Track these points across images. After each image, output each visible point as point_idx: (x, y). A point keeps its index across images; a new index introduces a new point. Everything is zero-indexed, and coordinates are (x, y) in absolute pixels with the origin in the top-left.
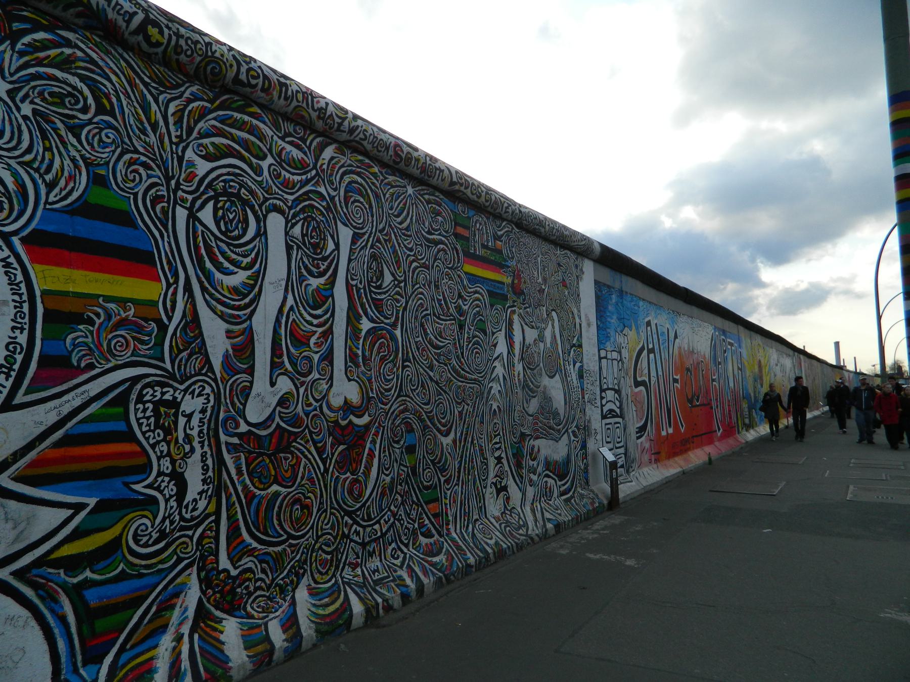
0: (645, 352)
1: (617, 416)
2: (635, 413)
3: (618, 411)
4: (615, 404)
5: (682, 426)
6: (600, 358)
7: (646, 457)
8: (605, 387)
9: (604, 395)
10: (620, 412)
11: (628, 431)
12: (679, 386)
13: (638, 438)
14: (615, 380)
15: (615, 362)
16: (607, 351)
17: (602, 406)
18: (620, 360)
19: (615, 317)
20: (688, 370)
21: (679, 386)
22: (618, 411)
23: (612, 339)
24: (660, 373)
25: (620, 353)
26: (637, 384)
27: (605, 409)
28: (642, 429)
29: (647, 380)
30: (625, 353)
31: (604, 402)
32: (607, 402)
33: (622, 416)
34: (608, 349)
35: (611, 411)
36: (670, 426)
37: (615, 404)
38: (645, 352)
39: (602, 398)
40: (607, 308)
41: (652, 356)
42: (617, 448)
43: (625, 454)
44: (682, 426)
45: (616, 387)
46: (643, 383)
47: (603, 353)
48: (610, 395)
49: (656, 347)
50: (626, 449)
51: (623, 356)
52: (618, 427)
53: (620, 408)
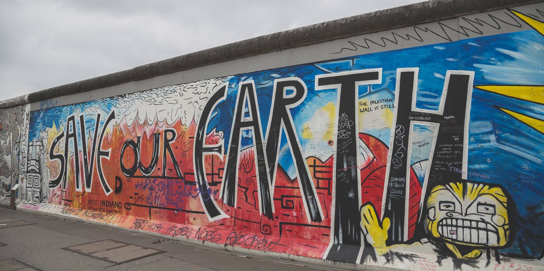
0: (64, 138)
1: (37, 173)
2: (49, 173)
3: (37, 171)
4: (36, 167)
5: (108, 190)
6: (29, 146)
7: (57, 200)
8: (30, 158)
9: (29, 162)
10: (39, 171)
11: (43, 181)
12: (108, 158)
13: (50, 187)
14: (37, 156)
15: (38, 147)
16: (33, 142)
17: (28, 167)
18: (42, 145)
19: (41, 124)
20: (132, 142)
21: (108, 158)
22: (37, 171)
23: (37, 136)
24: (80, 148)
25: (42, 142)
26: (52, 157)
27: (29, 169)
28: (54, 183)
29: (64, 155)
30: (45, 141)
31: (29, 165)
32: (31, 166)
33: (40, 173)
34: (34, 141)
35: (32, 170)
36: (88, 186)
37: (36, 167)
38: (64, 138)
39: (28, 164)
40: (36, 121)
41: (71, 139)
42: (34, 188)
43: (40, 193)
44: (108, 190)
45: (37, 159)
46: (60, 157)
47: (31, 143)
48: (33, 162)
49: (78, 131)
50: (41, 190)
51: (44, 143)
52: (37, 178)
53: (39, 169)
